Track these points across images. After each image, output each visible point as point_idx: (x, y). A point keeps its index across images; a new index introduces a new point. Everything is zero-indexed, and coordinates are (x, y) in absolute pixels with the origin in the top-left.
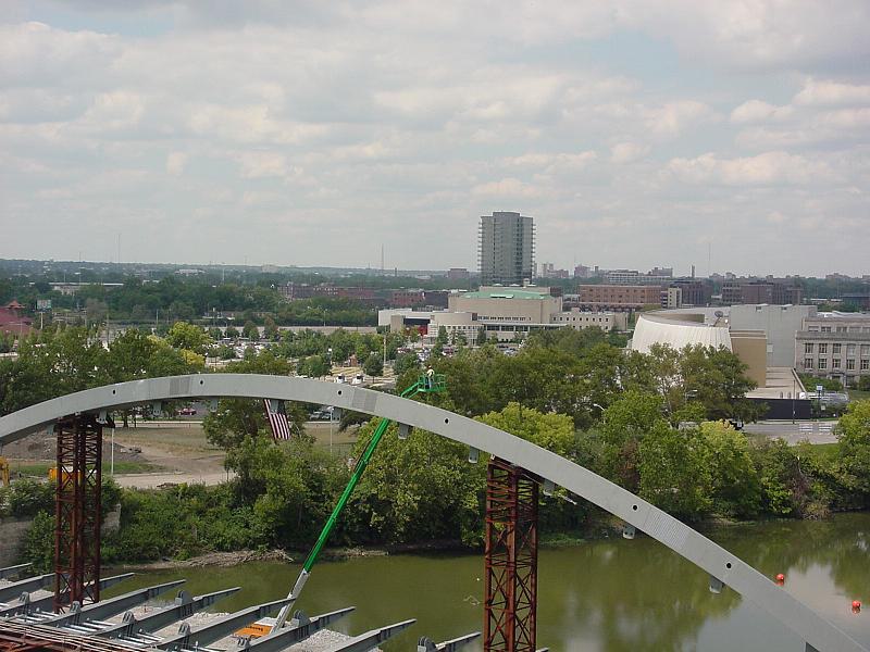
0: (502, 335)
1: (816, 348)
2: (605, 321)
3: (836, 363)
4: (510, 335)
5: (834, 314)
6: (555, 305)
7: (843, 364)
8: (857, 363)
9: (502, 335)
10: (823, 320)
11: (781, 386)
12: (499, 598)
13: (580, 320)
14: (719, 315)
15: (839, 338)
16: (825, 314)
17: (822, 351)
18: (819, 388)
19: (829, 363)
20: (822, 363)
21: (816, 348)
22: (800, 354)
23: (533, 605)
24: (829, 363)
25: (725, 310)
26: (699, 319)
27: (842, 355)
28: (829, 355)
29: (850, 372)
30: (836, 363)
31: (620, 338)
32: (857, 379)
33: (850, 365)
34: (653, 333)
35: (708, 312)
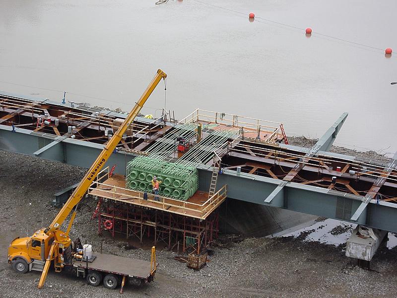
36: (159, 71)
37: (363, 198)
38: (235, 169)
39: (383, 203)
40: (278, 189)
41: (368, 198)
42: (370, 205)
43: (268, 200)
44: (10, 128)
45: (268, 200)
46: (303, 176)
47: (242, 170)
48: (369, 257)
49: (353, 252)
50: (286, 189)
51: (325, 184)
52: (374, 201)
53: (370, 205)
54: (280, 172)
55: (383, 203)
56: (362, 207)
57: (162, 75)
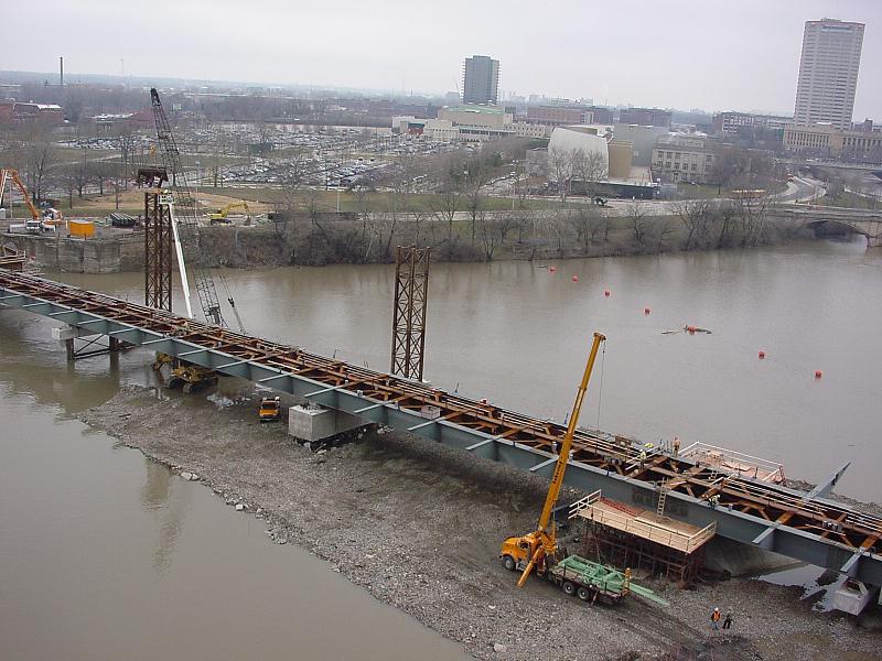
1: (665, 155)
2: (537, 132)
4: (476, 137)
11: (640, 178)
12: (404, 296)
14: (608, 129)
15: (677, 148)
19: (673, 165)
20: (668, 165)
21: (665, 155)
22: (655, 159)
23: (425, 300)
24: (673, 165)
25: (612, 128)
26: (594, 132)
27: (683, 159)
28: (673, 161)
31: (543, 144)
32: (689, 177)
35: (602, 129)
36: (596, 335)
37: (855, 549)
38: (727, 506)
39: (875, 556)
40: (770, 530)
41: (862, 550)
42: (862, 557)
43: (756, 541)
44: (511, 443)
45: (756, 541)
46: (796, 520)
47: (734, 508)
48: (856, 612)
49: (840, 604)
50: (776, 531)
51: (818, 532)
52: (867, 554)
53: (862, 557)
54: (774, 514)
55: (875, 556)
56: (855, 558)
57: (600, 338)
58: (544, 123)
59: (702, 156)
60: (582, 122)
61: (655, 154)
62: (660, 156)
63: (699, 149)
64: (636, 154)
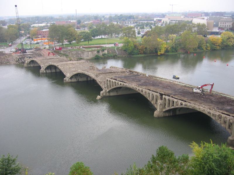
0: (173, 22)
3: (225, 26)
4: (174, 22)
5: (226, 18)
6: (182, 17)
7: (226, 26)
8: (229, 26)
9: (173, 22)
10: (224, 19)
11: (216, 30)
13: (186, 19)
14: (207, 18)
16: (224, 18)
17: (223, 23)
18: (220, 30)
20: (223, 26)
25: (208, 17)
26: (204, 19)
28: (224, 25)
29: (227, 27)
30: (225, 26)
33: (227, 26)
34: (196, 21)
35: (206, 18)
58: (192, 17)
59: (232, 23)
60: (201, 16)
61: (220, 23)
62: (221, 24)
63: (231, 21)
64: (215, 23)
